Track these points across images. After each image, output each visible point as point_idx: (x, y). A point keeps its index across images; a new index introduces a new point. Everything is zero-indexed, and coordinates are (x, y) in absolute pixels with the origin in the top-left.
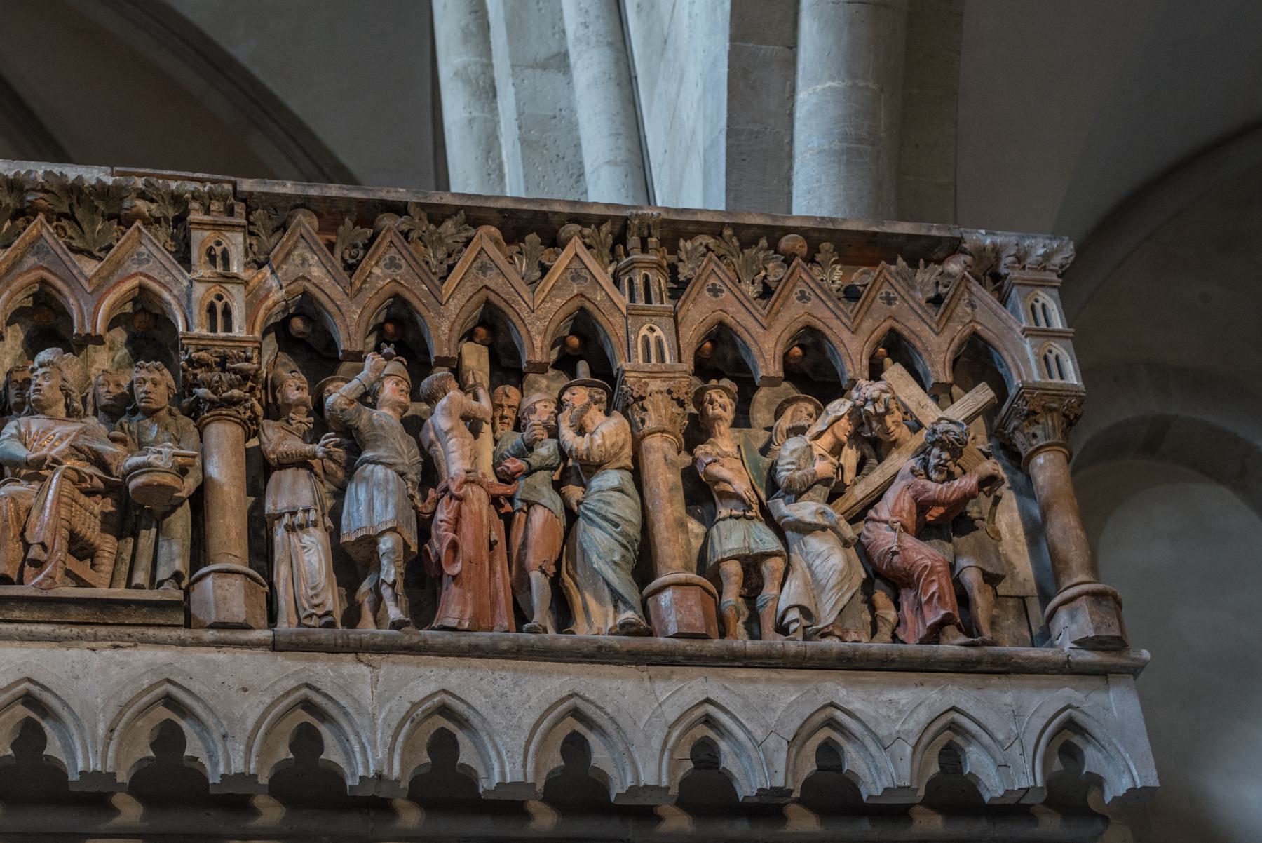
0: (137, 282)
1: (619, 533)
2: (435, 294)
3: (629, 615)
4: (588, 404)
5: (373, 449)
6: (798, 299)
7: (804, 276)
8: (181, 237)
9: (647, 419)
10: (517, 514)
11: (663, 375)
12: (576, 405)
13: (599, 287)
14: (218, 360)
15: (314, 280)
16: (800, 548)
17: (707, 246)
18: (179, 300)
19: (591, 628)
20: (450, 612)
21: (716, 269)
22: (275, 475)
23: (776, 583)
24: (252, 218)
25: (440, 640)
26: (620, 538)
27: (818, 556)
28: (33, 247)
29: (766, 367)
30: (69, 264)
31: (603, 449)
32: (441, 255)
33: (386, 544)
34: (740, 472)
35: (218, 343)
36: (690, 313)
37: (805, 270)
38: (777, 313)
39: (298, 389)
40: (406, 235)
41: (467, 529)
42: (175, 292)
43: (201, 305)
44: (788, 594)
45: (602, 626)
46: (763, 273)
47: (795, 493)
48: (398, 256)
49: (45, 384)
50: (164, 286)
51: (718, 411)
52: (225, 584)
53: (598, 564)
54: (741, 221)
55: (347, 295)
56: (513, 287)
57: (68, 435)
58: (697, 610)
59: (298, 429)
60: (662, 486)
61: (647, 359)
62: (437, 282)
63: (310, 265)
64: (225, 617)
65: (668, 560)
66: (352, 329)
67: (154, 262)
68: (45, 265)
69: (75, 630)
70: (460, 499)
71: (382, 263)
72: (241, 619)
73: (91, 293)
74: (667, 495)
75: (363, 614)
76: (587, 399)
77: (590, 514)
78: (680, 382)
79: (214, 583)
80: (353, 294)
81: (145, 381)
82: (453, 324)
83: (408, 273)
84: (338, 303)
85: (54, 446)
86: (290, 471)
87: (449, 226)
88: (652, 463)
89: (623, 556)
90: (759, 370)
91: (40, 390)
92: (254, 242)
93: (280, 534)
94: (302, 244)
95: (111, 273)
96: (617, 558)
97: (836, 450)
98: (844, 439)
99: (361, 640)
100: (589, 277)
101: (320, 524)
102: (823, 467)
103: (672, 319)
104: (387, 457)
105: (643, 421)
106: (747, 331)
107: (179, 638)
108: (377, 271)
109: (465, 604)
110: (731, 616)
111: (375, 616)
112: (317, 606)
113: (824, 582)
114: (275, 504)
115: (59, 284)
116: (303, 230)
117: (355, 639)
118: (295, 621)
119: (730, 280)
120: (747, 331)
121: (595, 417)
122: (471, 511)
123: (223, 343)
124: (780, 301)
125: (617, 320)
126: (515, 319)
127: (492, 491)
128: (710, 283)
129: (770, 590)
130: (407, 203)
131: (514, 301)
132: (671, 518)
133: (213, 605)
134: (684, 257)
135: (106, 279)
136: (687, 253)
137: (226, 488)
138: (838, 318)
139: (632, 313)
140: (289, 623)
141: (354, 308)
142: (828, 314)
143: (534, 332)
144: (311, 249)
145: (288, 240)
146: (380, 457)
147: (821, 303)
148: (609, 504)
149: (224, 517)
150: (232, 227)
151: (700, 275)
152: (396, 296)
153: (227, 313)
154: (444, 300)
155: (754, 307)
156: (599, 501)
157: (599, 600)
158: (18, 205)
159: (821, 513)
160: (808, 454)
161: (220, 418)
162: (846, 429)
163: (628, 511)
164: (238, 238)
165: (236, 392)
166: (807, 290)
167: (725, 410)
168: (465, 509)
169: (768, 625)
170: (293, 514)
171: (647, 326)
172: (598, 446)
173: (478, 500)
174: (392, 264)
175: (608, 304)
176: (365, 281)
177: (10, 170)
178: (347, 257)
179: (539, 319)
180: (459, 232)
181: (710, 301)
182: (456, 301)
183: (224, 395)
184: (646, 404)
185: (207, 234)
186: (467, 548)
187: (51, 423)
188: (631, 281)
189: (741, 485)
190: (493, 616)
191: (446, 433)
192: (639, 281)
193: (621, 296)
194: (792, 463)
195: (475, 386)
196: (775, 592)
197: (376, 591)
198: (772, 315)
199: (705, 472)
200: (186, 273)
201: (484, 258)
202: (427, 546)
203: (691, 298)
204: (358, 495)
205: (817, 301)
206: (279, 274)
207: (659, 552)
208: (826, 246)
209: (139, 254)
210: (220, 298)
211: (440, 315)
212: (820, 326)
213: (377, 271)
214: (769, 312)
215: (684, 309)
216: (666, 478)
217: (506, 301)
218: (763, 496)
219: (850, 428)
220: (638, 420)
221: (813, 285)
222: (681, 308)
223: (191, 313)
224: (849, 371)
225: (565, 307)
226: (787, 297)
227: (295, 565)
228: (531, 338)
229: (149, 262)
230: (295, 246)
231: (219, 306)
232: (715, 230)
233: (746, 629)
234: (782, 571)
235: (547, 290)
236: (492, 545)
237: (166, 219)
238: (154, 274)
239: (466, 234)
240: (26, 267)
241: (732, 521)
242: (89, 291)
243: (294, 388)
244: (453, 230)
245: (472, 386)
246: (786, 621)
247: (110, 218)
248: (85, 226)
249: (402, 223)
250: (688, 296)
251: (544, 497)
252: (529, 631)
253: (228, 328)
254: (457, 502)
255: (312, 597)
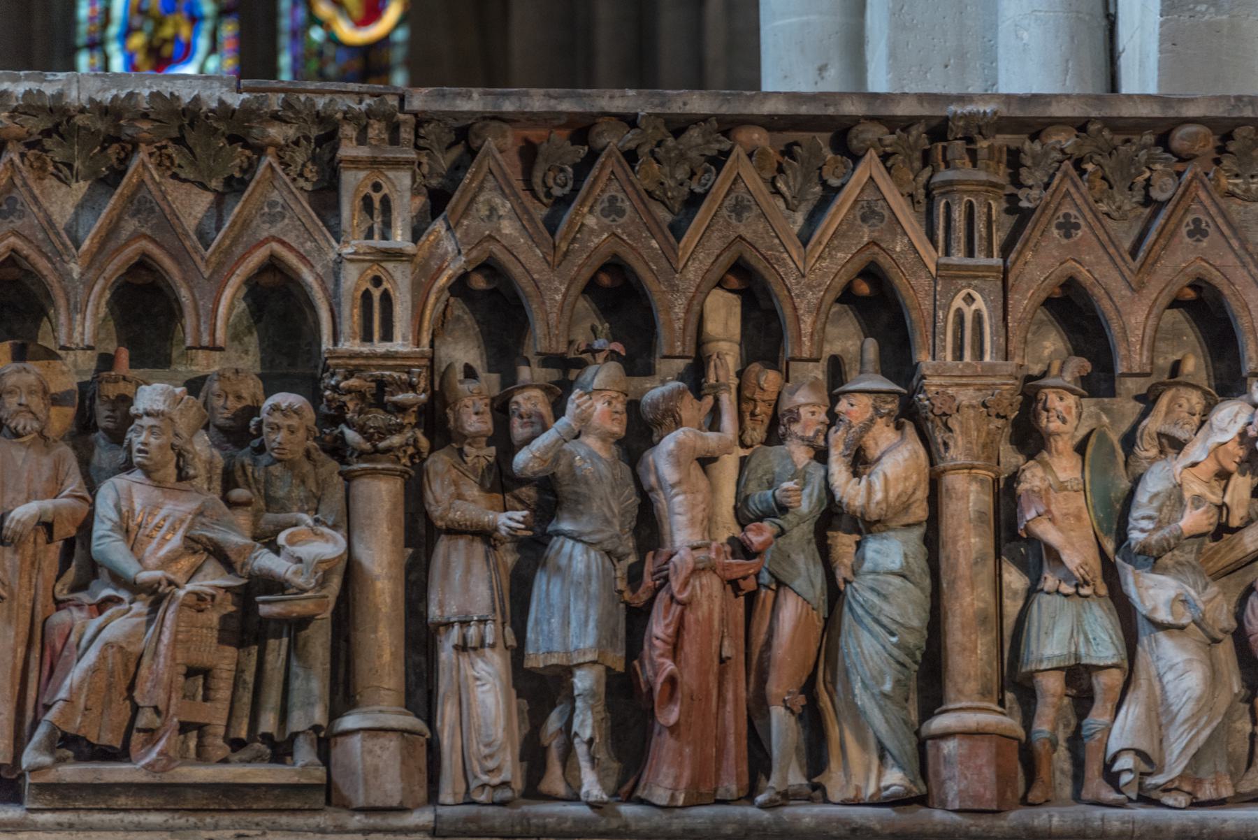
0: (268, 252)
1: (897, 645)
2: (670, 255)
3: (895, 779)
4: (872, 421)
5: (575, 515)
6: (1191, 234)
7: (1203, 195)
8: (327, 157)
9: (951, 444)
10: (763, 590)
11: (978, 381)
12: (854, 422)
13: (899, 231)
14: (373, 385)
15: (504, 242)
16: (1150, 644)
17: (1062, 151)
18: (323, 282)
19: (848, 782)
20: (661, 777)
21: (1072, 190)
22: (443, 545)
23: (1109, 706)
24: (422, 131)
25: (645, 824)
26: (896, 652)
27: (1171, 668)
28: (131, 202)
29: (1128, 358)
30: (180, 230)
31: (884, 506)
32: (681, 174)
33: (583, 681)
34: (1078, 518)
35: (374, 362)
36: (1028, 269)
37: (1205, 186)
38: (1156, 262)
39: (477, 414)
40: (631, 157)
41: (690, 648)
42: (319, 269)
43: (354, 299)
44: (1122, 729)
45: (862, 784)
46: (1147, 174)
47: (1151, 558)
48: (620, 195)
49: (152, 440)
50: (303, 258)
51: (1055, 425)
52: (377, 748)
53: (863, 699)
54: (1115, 114)
55: (547, 262)
56: (778, 237)
57: (182, 521)
58: (989, 773)
59: (474, 469)
60: (962, 560)
61: (958, 353)
62: (672, 240)
63: (500, 217)
64: (377, 800)
65: (960, 680)
66: (553, 318)
67: (291, 218)
68: (149, 232)
69: (193, 820)
70: (684, 604)
71: (598, 208)
72: (395, 802)
73: (209, 279)
74: (967, 573)
75: (550, 764)
76: (871, 411)
77: (860, 611)
78: (1001, 394)
79: (363, 746)
80: (556, 260)
81: (279, 428)
82: (690, 304)
83: (633, 221)
84: (536, 276)
85: (164, 540)
86: (462, 542)
87: (694, 134)
88: (952, 516)
89: (898, 682)
90: (1119, 362)
91: (146, 452)
92: (425, 160)
93: (446, 654)
94: (491, 182)
95: (235, 241)
96: (888, 687)
97: (1223, 476)
98: (1232, 467)
99: (545, 826)
100: (886, 213)
101: (500, 644)
102: (1192, 520)
103: (999, 283)
104: (590, 533)
105: (946, 444)
106: (1107, 293)
107: (318, 826)
108: (591, 221)
109: (680, 765)
110: (1043, 752)
111: (564, 766)
112: (489, 772)
113: (1175, 708)
114: (441, 606)
115: (167, 263)
116: (492, 164)
117: (538, 826)
118: (461, 788)
119: (1091, 209)
120: (1107, 293)
121: (883, 437)
122: (697, 621)
123: (381, 362)
124: (1162, 241)
125: (922, 283)
126: (776, 288)
127: (728, 575)
128: (1060, 213)
129: (1097, 717)
130: (636, 115)
131: (777, 260)
132: (970, 612)
133: (361, 781)
134: (1029, 163)
135: (228, 252)
136: (1034, 157)
137: (379, 585)
138: (1244, 265)
139: (949, 275)
140: (455, 794)
141: (557, 283)
142: (1231, 259)
143: (802, 307)
144: (502, 189)
145: (471, 181)
146: (581, 534)
147: (1222, 241)
148: (885, 597)
149: (375, 631)
150: (396, 164)
151: (1048, 204)
152: (615, 255)
153: (386, 298)
154: (681, 266)
155: (1121, 256)
156: (872, 589)
157: (863, 743)
158: (112, 132)
159: (1184, 601)
160: (1176, 498)
161: (373, 473)
162: (1235, 456)
163: (910, 609)
164: (403, 179)
165: (396, 440)
166: (1204, 218)
167: (1064, 421)
168: (690, 617)
169: (1093, 770)
170: (465, 623)
171: (964, 293)
172: (878, 503)
173: (709, 594)
174: (613, 209)
175: (911, 257)
176: (574, 240)
177: (105, 90)
178: (550, 182)
179: (810, 287)
180: (708, 142)
181: (1060, 246)
182: (697, 264)
183: (382, 445)
184: (952, 423)
185: (362, 175)
186: (688, 680)
187: (157, 493)
188: (948, 207)
189: (1072, 559)
190: (718, 770)
191: (673, 486)
192: (958, 215)
193: (930, 247)
194: (1150, 518)
195: (717, 388)
196: (1106, 719)
197: (567, 731)
198: (1148, 267)
199: (1026, 529)
200: (334, 243)
201: (740, 190)
202: (636, 663)
203: (1031, 244)
204: (546, 589)
205: (1217, 236)
206: (458, 235)
207: (950, 663)
208: (1240, 132)
209: (272, 204)
210: (377, 281)
211: (673, 288)
212: (1217, 279)
213: (591, 221)
214: (1142, 265)
215: (1020, 263)
216: (969, 544)
217: (767, 260)
218: (1110, 546)
219: (1241, 453)
220: (940, 440)
221: (1213, 210)
222: (1014, 263)
223: (339, 304)
224: (1250, 359)
225: (849, 266)
226: (1173, 234)
227: (464, 706)
228: (798, 319)
229: (284, 217)
230: (481, 188)
231: (376, 294)
232: (1081, 126)
233: (1069, 749)
234: (1118, 690)
235: (825, 241)
236: (722, 661)
237: (307, 138)
238: (290, 239)
239: (717, 146)
240: (124, 235)
241: (1058, 599)
242: (206, 276)
243: (471, 410)
244: (700, 141)
245: (713, 387)
246: (1116, 767)
247: (233, 139)
248: (198, 151)
249: (630, 138)
250: (1027, 241)
251: (799, 574)
252: (763, 807)
253: (387, 336)
254: (679, 608)
255: (485, 757)
